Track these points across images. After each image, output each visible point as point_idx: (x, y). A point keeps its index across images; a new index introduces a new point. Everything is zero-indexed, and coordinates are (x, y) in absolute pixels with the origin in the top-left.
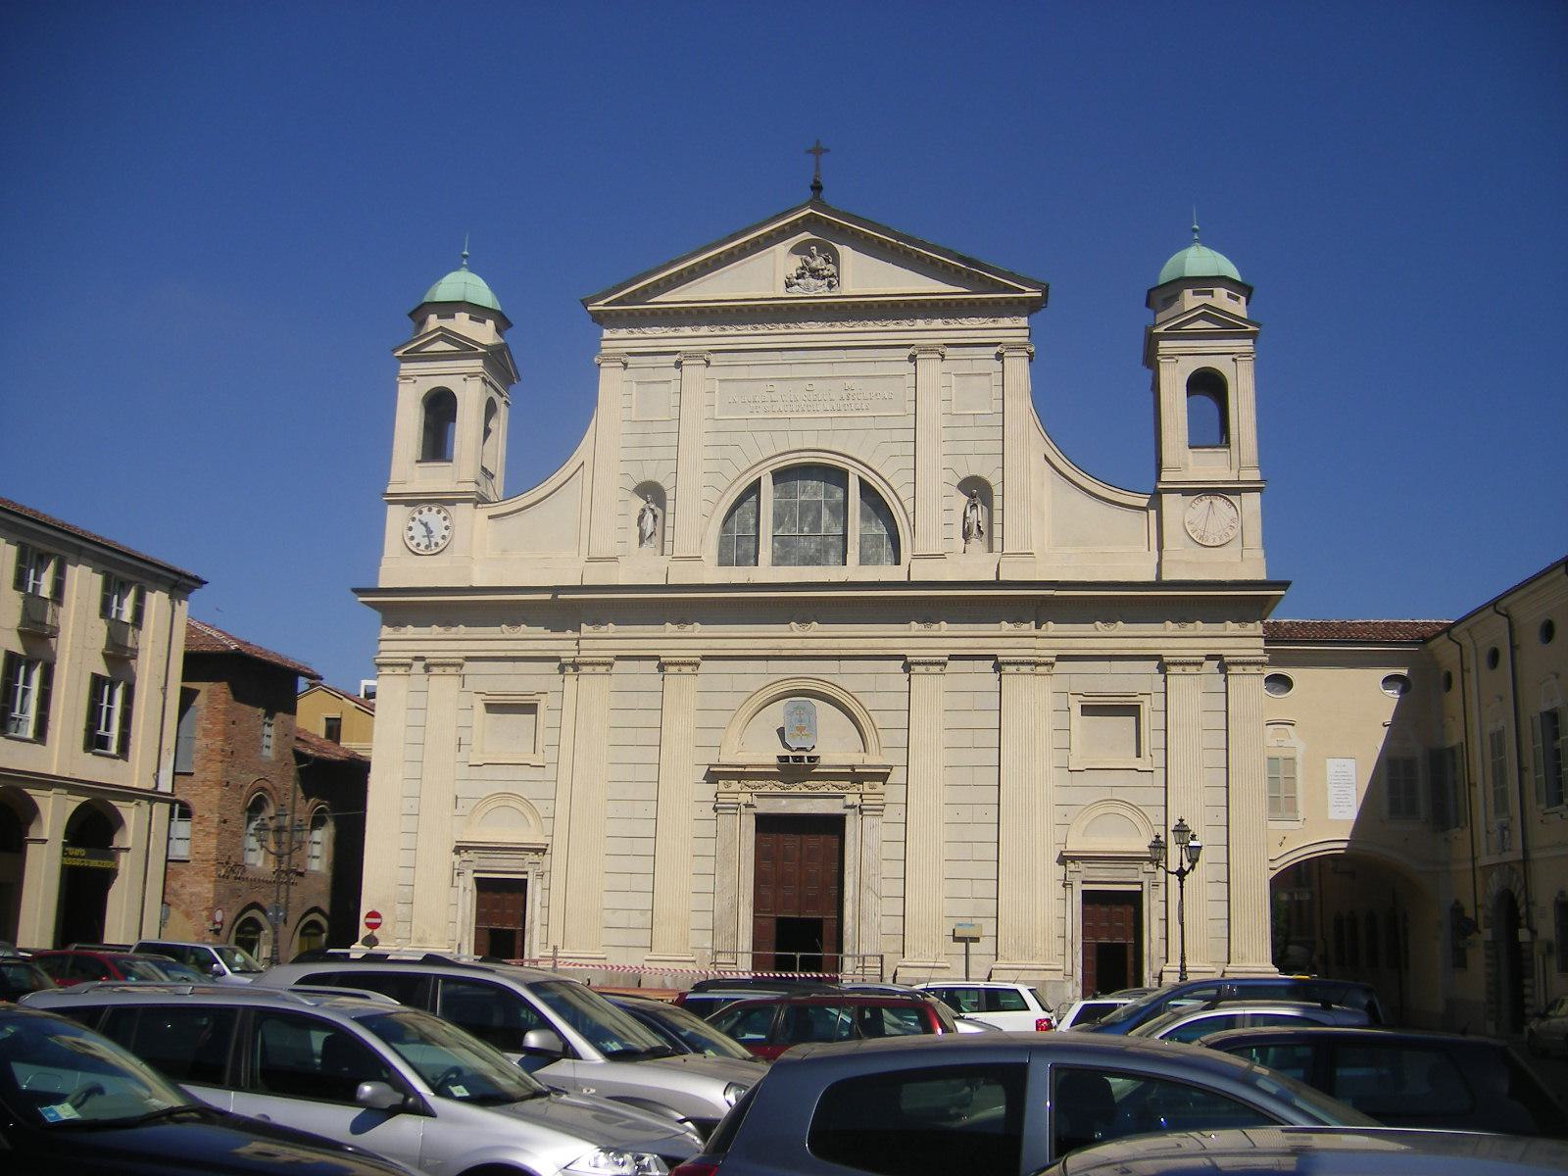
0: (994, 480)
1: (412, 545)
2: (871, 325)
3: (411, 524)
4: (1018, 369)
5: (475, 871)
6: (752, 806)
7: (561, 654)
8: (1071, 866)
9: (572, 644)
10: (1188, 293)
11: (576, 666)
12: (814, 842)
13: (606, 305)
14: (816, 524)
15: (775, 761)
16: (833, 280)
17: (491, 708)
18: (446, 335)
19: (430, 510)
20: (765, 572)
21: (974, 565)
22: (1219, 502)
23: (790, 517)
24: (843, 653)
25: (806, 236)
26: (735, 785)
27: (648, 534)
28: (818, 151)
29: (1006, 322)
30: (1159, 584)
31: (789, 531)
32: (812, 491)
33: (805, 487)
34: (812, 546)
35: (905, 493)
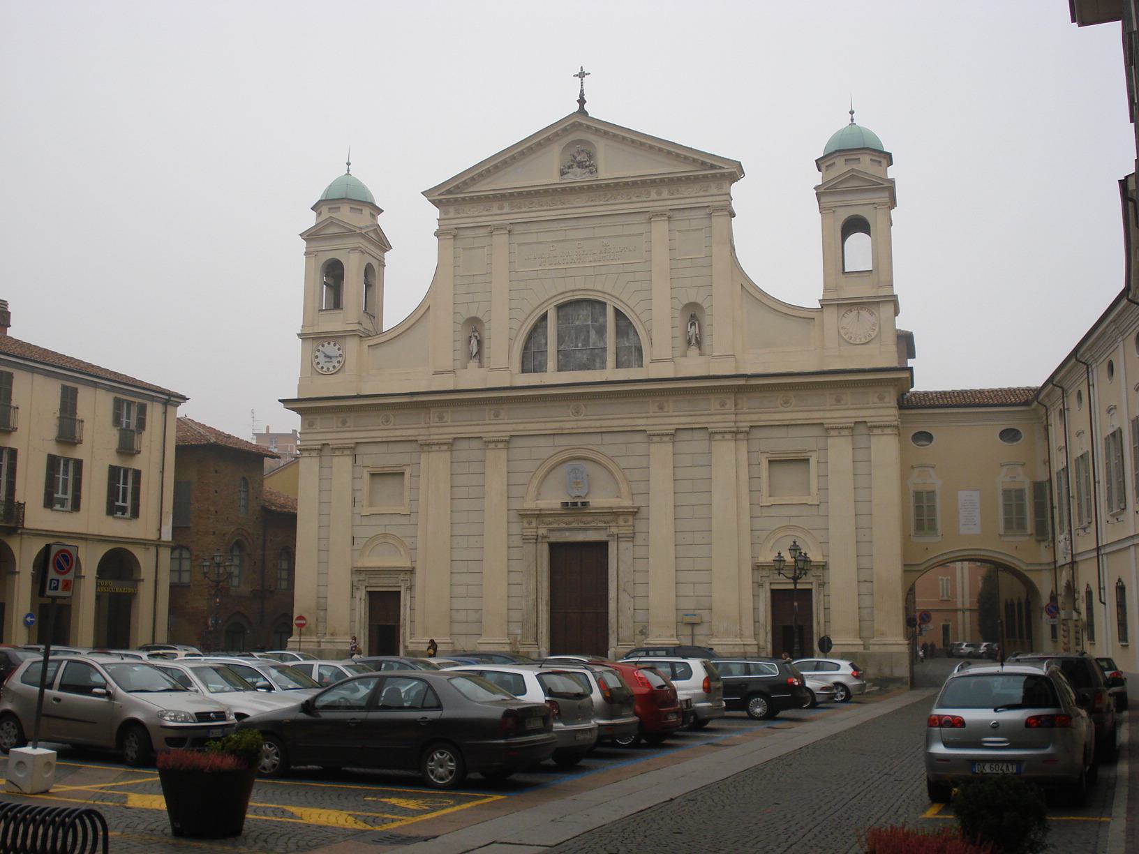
1: (318, 368)
3: (317, 354)
14: (587, 341)
15: (559, 506)
16: (593, 169)
19: (329, 343)
20: (552, 376)
21: (693, 365)
22: (864, 313)
23: (569, 337)
24: (604, 430)
27: (473, 355)
28: (582, 75)
31: (569, 347)
32: (583, 317)
33: (579, 315)
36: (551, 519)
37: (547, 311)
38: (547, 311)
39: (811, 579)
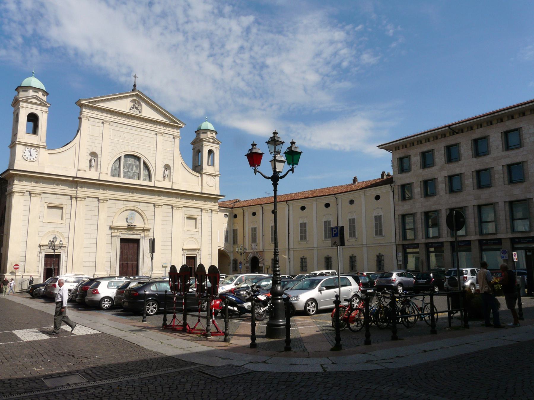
0: (171, 165)
1: (25, 158)
2: (148, 124)
4: (177, 141)
5: (45, 252)
6: (120, 236)
7: (155, 202)
8: (184, 251)
9: (75, 192)
10: (209, 132)
11: (76, 198)
12: (131, 245)
13: (86, 102)
14: (132, 169)
15: (127, 226)
17: (49, 207)
18: (36, 98)
20: (122, 180)
21: (166, 184)
22: (212, 177)
24: (141, 201)
25: (135, 98)
26: (116, 231)
29: (175, 130)
30: (201, 193)
32: (131, 161)
34: (131, 174)
35: (154, 165)
36: (122, 231)
37: (121, 156)
38: (121, 156)
39: (197, 254)
